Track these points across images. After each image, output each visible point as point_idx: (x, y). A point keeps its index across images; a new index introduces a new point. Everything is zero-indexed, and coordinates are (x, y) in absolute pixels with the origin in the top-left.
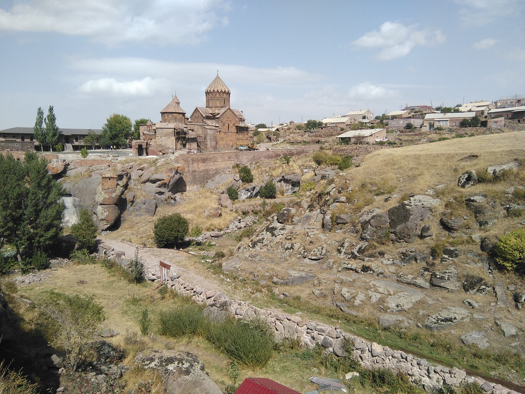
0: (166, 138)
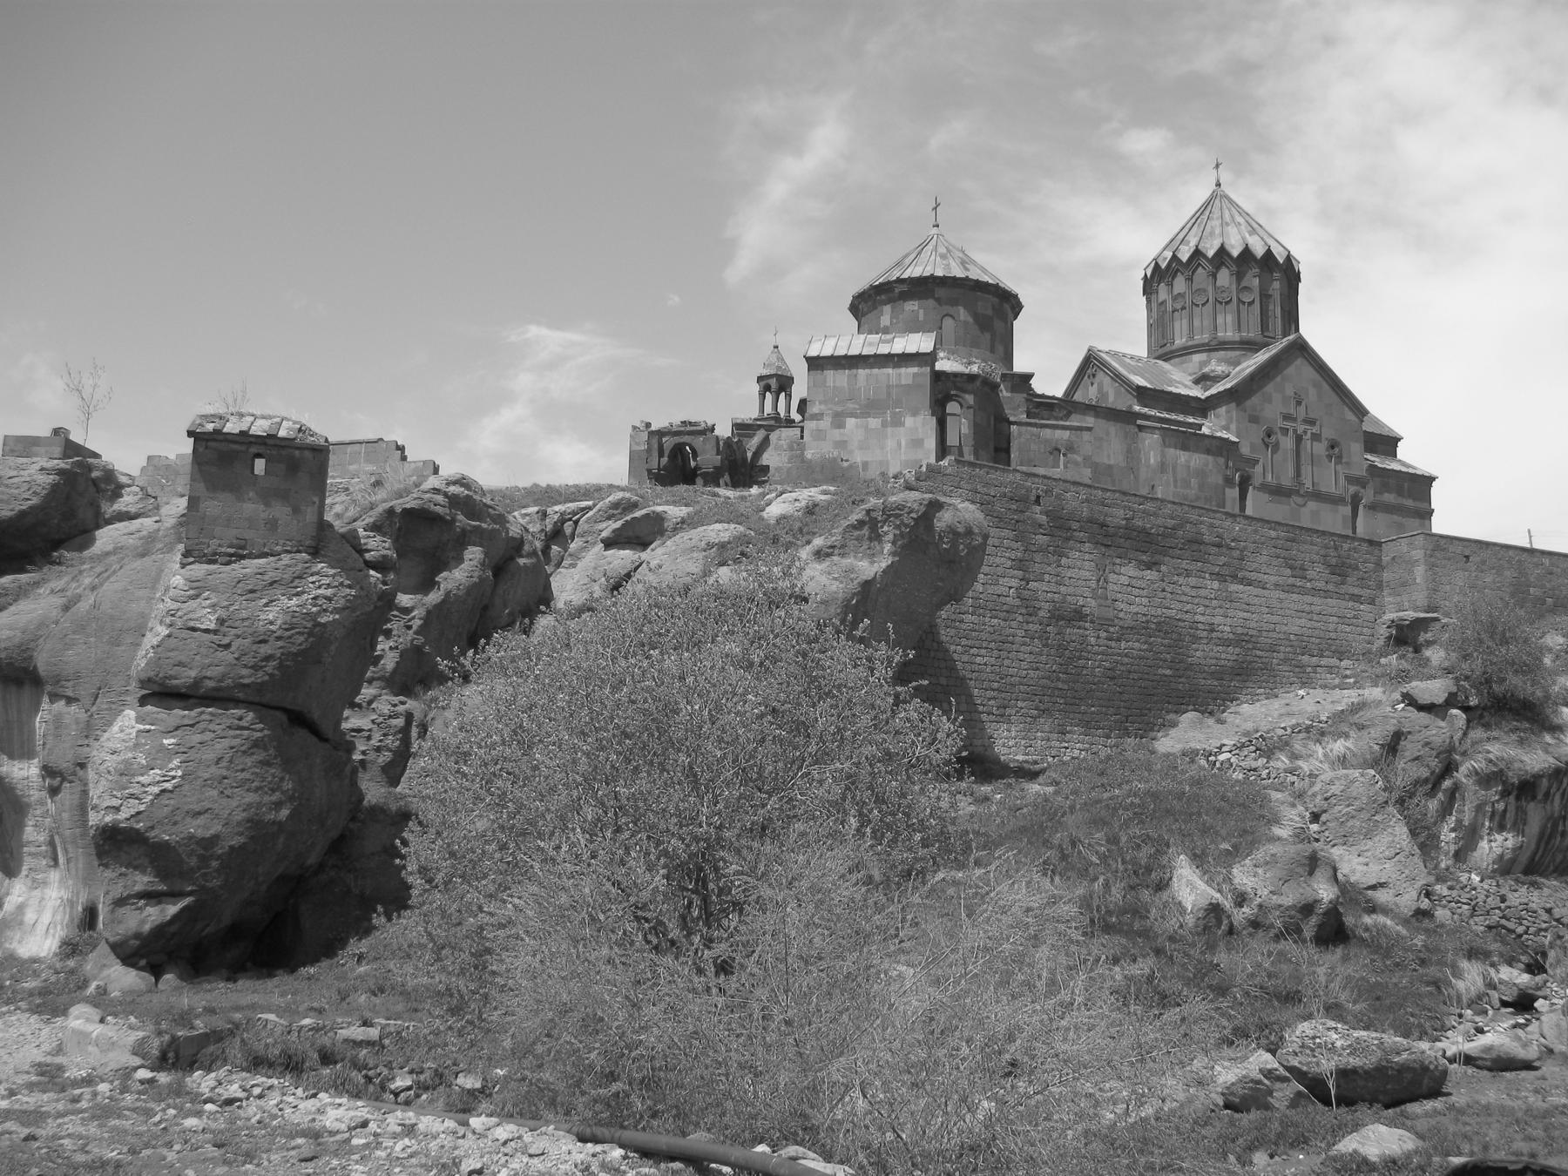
0: (874, 423)
